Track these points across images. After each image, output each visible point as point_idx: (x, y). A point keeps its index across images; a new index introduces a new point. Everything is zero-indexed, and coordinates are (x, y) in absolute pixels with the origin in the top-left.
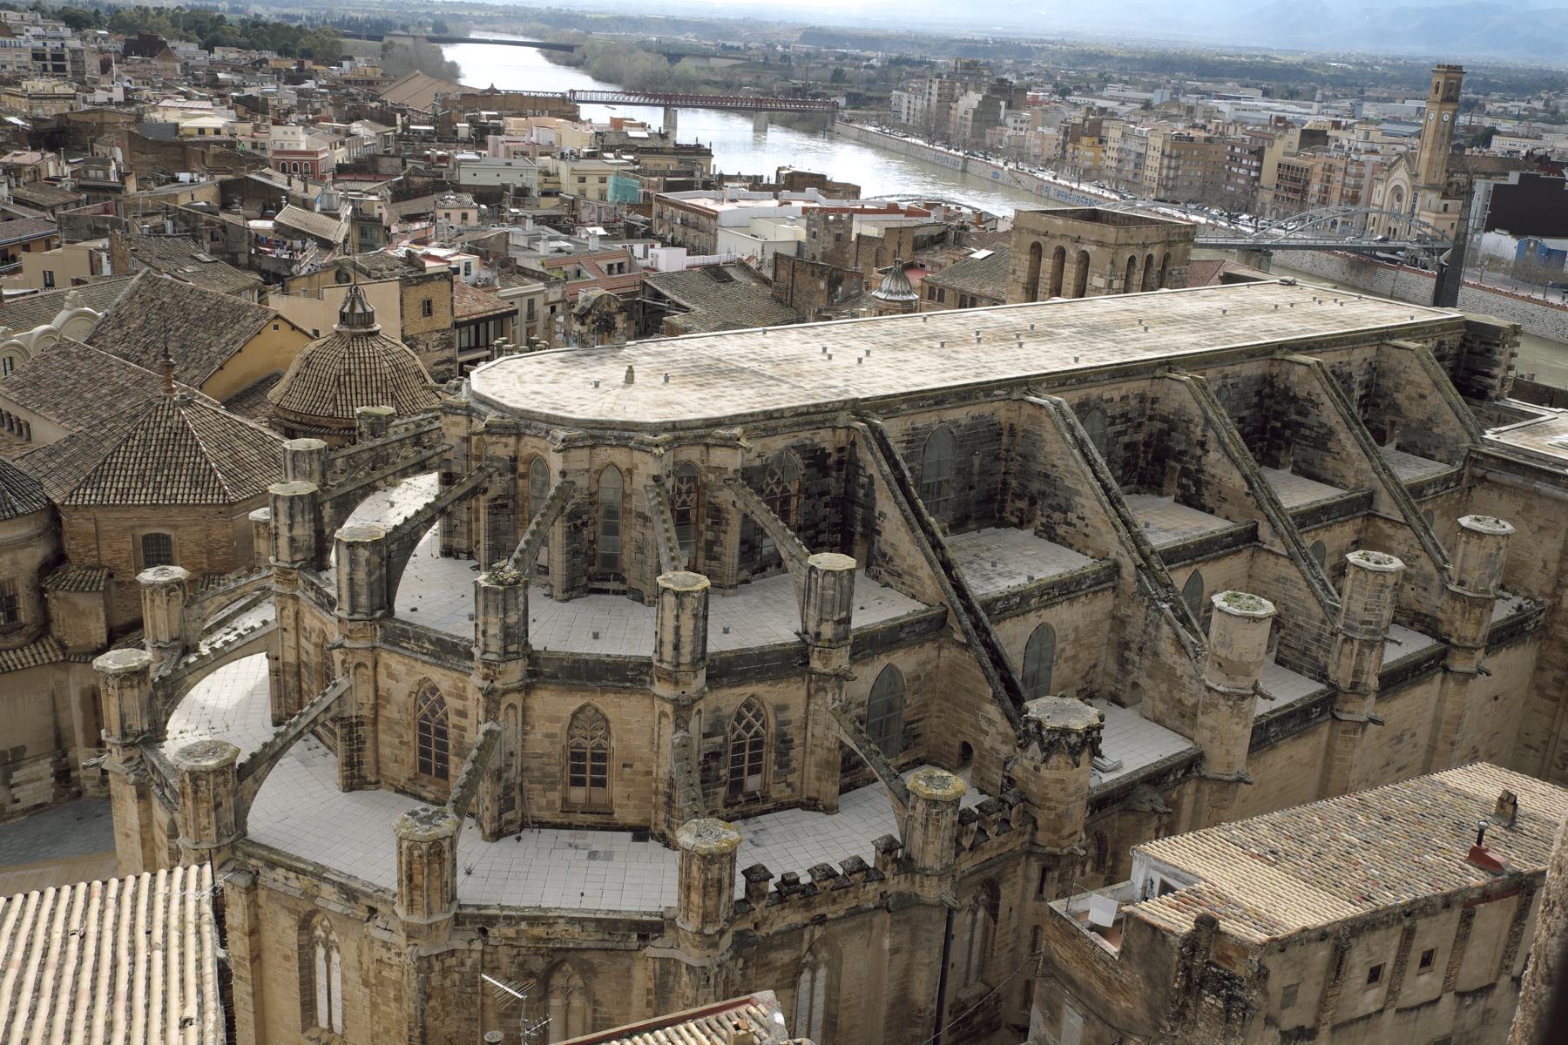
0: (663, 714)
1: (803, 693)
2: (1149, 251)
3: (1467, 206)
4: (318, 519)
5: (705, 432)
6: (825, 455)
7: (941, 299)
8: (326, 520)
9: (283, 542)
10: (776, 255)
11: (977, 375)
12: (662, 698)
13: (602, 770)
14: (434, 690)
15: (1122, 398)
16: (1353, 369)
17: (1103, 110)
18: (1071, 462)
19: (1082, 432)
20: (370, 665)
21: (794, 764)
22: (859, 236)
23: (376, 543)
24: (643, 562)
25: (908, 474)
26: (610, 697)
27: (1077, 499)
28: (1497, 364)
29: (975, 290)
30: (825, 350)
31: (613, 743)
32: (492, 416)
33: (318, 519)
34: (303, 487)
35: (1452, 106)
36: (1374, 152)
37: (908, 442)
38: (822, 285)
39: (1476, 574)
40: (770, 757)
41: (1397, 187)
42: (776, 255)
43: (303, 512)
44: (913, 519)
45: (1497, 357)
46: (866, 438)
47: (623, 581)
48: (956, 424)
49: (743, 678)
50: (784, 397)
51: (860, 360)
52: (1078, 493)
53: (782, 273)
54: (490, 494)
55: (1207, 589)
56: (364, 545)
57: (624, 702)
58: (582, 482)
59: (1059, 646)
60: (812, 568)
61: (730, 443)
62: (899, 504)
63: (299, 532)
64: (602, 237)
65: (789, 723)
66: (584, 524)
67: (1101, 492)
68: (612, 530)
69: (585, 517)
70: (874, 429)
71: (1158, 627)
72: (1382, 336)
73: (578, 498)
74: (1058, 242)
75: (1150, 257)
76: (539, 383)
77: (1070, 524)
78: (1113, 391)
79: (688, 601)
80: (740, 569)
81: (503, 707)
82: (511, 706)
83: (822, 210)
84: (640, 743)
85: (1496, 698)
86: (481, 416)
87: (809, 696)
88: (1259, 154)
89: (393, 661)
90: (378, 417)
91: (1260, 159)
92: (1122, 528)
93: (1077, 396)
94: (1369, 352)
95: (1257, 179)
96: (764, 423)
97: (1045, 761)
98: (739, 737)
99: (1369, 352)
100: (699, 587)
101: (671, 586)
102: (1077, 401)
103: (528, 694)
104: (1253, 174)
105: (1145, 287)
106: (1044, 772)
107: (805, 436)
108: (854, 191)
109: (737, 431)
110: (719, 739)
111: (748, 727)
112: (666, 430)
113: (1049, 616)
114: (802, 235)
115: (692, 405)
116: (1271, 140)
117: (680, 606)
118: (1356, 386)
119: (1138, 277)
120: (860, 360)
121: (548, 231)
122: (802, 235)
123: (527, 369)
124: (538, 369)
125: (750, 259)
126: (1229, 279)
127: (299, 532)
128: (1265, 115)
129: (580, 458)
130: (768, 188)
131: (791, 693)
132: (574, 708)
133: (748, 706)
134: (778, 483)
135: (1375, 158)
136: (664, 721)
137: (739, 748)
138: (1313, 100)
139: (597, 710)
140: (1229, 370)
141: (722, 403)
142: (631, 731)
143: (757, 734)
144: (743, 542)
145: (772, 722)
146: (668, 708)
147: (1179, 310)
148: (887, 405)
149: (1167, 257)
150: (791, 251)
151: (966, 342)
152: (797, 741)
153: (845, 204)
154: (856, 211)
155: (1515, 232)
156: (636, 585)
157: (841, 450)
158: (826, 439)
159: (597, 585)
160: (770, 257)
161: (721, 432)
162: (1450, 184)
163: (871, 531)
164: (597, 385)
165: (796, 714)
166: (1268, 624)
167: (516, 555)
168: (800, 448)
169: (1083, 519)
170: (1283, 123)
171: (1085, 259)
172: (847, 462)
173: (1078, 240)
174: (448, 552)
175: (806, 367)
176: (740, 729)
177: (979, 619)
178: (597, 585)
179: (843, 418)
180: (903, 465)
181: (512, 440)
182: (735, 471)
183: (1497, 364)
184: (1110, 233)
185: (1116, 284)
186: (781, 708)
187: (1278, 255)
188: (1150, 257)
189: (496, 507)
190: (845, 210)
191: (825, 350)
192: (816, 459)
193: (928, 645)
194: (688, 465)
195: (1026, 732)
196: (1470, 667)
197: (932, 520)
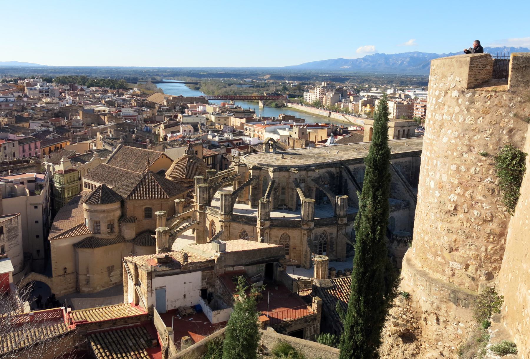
0: (305, 234)
1: (336, 230)
2: (404, 128)
4: (209, 193)
5: (307, 168)
8: (211, 193)
12: (304, 229)
13: (288, 250)
14: (245, 231)
15: (405, 162)
17: (372, 96)
18: (395, 176)
20: (228, 226)
21: (334, 249)
23: (231, 195)
24: (293, 200)
26: (291, 230)
27: (397, 185)
31: (291, 243)
33: (209, 193)
40: (328, 247)
43: (206, 191)
46: (344, 169)
47: (287, 206)
49: (322, 225)
50: (321, 161)
52: (397, 184)
54: (253, 185)
56: (228, 195)
57: (294, 232)
58: (277, 180)
59: (396, 223)
61: (313, 170)
62: (354, 185)
63: (205, 196)
65: (333, 238)
67: (404, 184)
68: (283, 193)
75: (404, 130)
78: (403, 160)
79: (311, 204)
81: (265, 233)
82: (267, 233)
84: (297, 242)
87: (338, 231)
89: (235, 225)
90: (213, 172)
92: (410, 192)
96: (320, 166)
97: (398, 245)
98: (321, 242)
103: (270, 231)
106: (398, 248)
110: (317, 241)
111: (323, 239)
115: (301, 162)
117: (309, 205)
127: (205, 196)
129: (277, 173)
131: (332, 230)
132: (281, 234)
133: (323, 233)
134: (323, 181)
136: (304, 236)
137: (321, 245)
139: (287, 234)
141: (308, 162)
142: (295, 239)
143: (325, 241)
145: (329, 237)
146: (306, 232)
147: (415, 142)
149: (409, 130)
151: (362, 149)
152: (335, 243)
156: (290, 206)
157: (338, 173)
158: (333, 170)
159: (280, 207)
165: (335, 235)
168: (328, 172)
175: (324, 155)
176: (321, 240)
178: (280, 207)
181: (258, 171)
186: (331, 234)
188: (404, 130)
189: (254, 188)
195: (393, 238)
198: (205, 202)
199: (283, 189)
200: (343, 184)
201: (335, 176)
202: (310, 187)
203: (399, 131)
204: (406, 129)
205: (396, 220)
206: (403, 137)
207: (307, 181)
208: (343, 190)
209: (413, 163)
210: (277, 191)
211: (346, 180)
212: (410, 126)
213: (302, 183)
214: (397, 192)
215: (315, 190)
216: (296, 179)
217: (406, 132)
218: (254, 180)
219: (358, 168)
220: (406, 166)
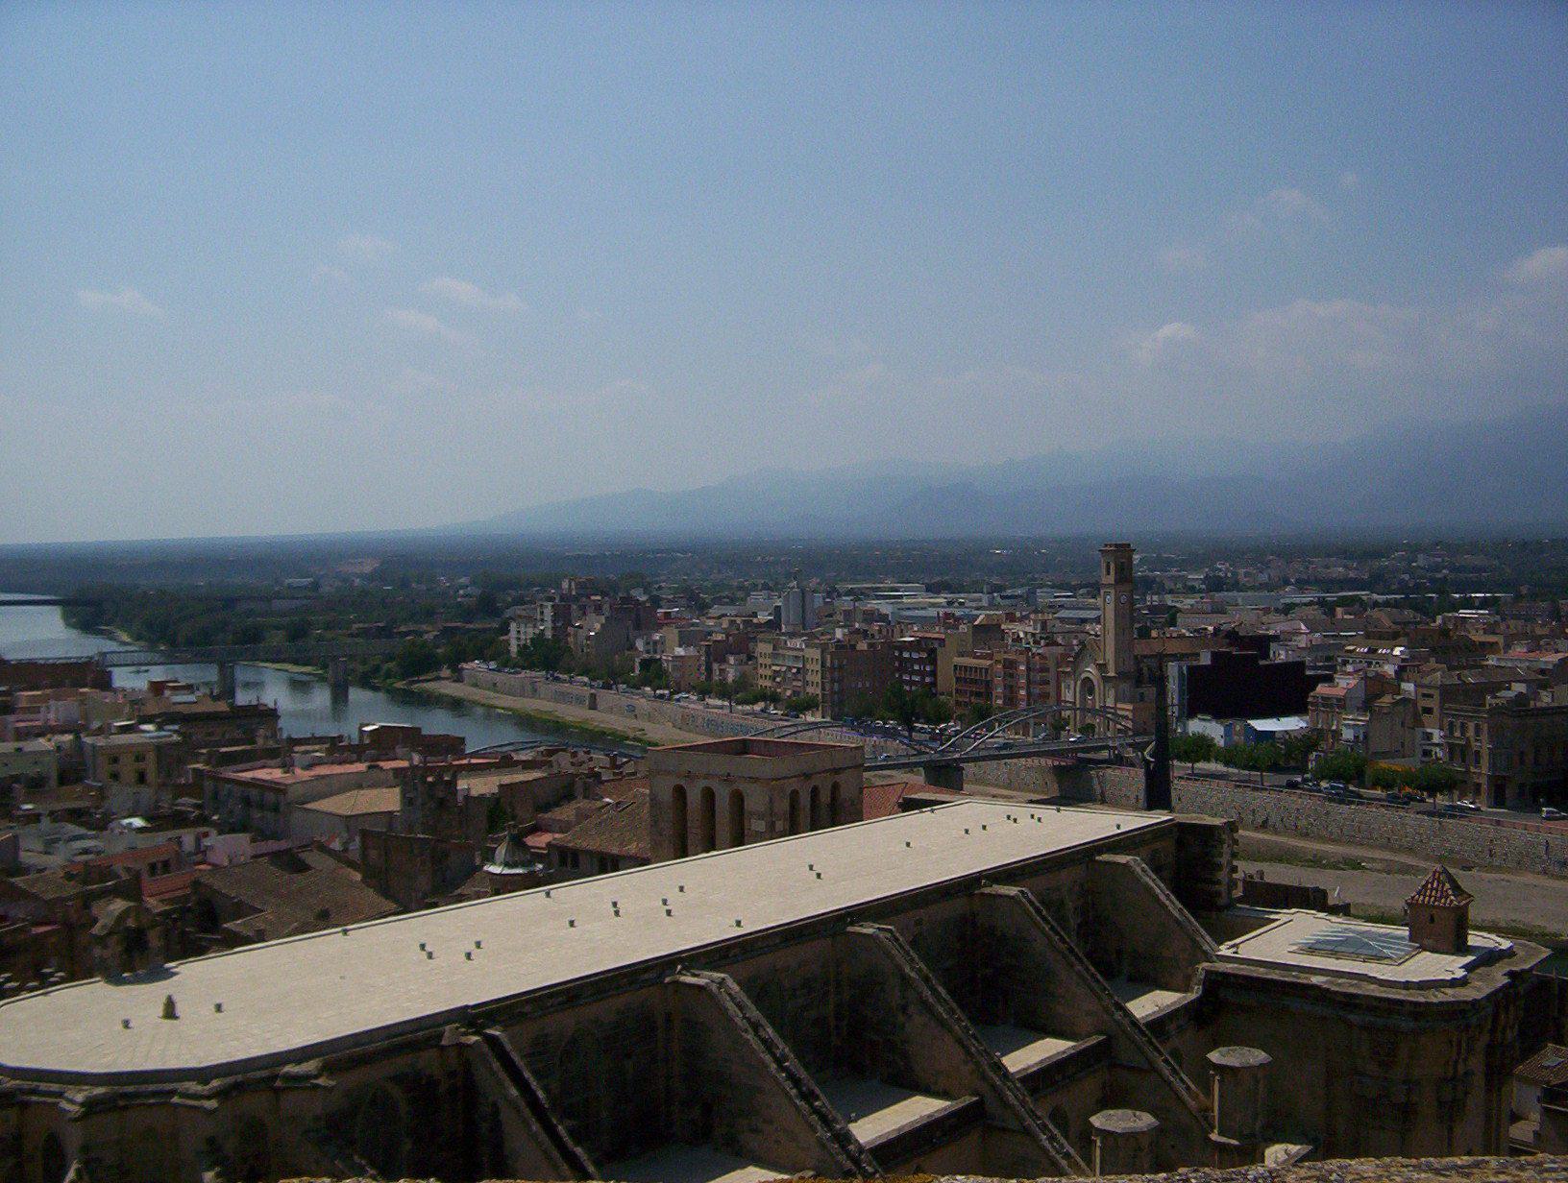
3: (1162, 692)
7: (576, 864)
25: (541, 1094)
28: (1219, 867)
29: (615, 851)
44: (556, 1154)
51: (468, 956)
53: (373, 854)
64: (140, 830)
70: (492, 1041)
74: (702, 783)
75: (815, 791)
95: (934, 684)
104: (928, 680)
105: (815, 825)
108: (455, 745)
109: (310, 1066)
119: (804, 816)
120: (468, 956)
121: (72, 829)
126: (909, 805)
130: (350, 748)
149: (835, 787)
155: (1218, 715)
157: (452, 1074)
158: (428, 1061)
168: (396, 1079)
171: (738, 799)
172: (466, 1088)
182: (317, 1118)
183: (1219, 867)
185: (779, 825)
187: (970, 768)
192: (420, 1088)
197: (579, 1150)
200: (484, 1126)
203: (795, 794)
211: (495, 1105)
216: (211, 1141)
217: (825, 797)
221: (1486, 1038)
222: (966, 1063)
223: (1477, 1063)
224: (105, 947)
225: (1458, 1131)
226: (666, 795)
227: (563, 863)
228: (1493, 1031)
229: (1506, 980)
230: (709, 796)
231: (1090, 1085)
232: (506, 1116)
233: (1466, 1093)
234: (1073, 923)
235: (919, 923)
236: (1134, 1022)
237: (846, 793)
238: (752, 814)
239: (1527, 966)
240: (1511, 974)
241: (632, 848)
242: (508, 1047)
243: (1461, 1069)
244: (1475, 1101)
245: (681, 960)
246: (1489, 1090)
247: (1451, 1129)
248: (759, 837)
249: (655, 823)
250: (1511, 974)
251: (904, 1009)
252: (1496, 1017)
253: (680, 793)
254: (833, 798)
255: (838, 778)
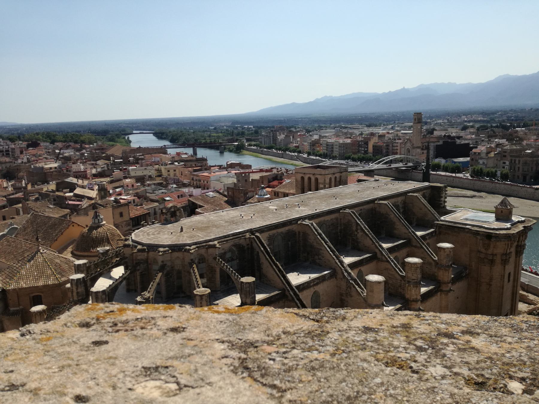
3: (428, 153)
6: (243, 247)
7: (278, 196)
9: (75, 294)
10: (228, 188)
11: (286, 217)
15: (331, 220)
16: (399, 203)
19: (320, 231)
22: (252, 179)
25: (269, 250)
28: (442, 197)
29: (287, 192)
30: (241, 215)
32: (139, 247)
34: (80, 276)
35: (419, 124)
36: (400, 139)
37: (268, 240)
38: (242, 195)
39: (445, 261)
41: (408, 149)
42: (228, 188)
45: (442, 195)
48: (282, 233)
51: (252, 217)
52: (321, 250)
53: (230, 193)
55: (364, 275)
58: (169, 264)
59: (321, 297)
60: (242, 282)
63: (79, 290)
66: (171, 277)
69: (171, 274)
70: (257, 237)
71: (350, 288)
72: (405, 193)
73: (168, 269)
74: (308, 176)
75: (336, 178)
76: (154, 234)
77: (320, 259)
78: (328, 218)
79: (204, 297)
80: (221, 285)
83: (240, 173)
85: (458, 298)
86: (136, 247)
88: (366, 143)
91: (367, 145)
93: (318, 220)
94: (403, 198)
95: (367, 150)
96: (222, 239)
99: (403, 198)
100: (207, 292)
101: (198, 293)
102: (318, 222)
104: (366, 149)
107: (237, 241)
108: (249, 167)
109: (216, 242)
112: (193, 245)
113: (317, 288)
114: (235, 181)
116: (369, 139)
118: (401, 208)
120: (252, 217)
122: (235, 181)
123: (151, 230)
124: (153, 230)
125: (220, 190)
126: (359, 181)
127: (79, 290)
128: (367, 132)
130: (224, 168)
135: (400, 141)
138: (380, 126)
140: (362, 207)
144: (221, 276)
148: (261, 230)
149: (341, 176)
150: (232, 186)
153: (247, 171)
154: (251, 172)
155: (445, 158)
157: (248, 245)
158: (242, 242)
160: (226, 188)
161: (211, 243)
162: (423, 146)
163: (260, 268)
164: (172, 233)
166: (383, 284)
167: (149, 289)
168: (235, 245)
169: (323, 257)
170: (372, 134)
171: (317, 180)
173: (314, 174)
174: (128, 290)
177: (295, 292)
179: (248, 235)
180: (267, 247)
183: (442, 197)
184: (323, 171)
185: (327, 186)
187: (376, 172)
190: (247, 172)
191: (241, 215)
192: (239, 247)
193: (281, 302)
194: (201, 255)
196: (448, 289)
197: (278, 263)
198: (80, 298)
199: (179, 272)
200: (256, 257)
201: (246, 248)
202: (212, 267)
204: (338, 175)
205: (321, 294)
206: (336, 186)
207: (208, 261)
208: (256, 264)
209: (341, 220)
210: (171, 277)
211: (258, 252)
212: (341, 173)
213: (203, 263)
214: (321, 258)
215: (218, 270)
217: (338, 179)
218: (141, 265)
219: (274, 235)
220: (332, 224)
221: (516, 244)
222: (372, 244)
223: (513, 250)
224: (167, 215)
225: (507, 267)
226: (299, 179)
227: (275, 195)
228: (518, 242)
229: (523, 228)
230: (310, 179)
231: (404, 251)
232: (261, 254)
233: (510, 258)
234: (401, 211)
235: (361, 210)
236: (417, 236)
237: (343, 178)
238: (320, 183)
239: (529, 225)
240: (524, 227)
241: (291, 191)
242: (261, 238)
243: (508, 251)
244: (512, 259)
245: (302, 218)
246: (516, 257)
247: (505, 267)
248: (322, 189)
249: (296, 186)
250: (524, 227)
251: (357, 231)
252: (519, 238)
253: (303, 178)
254: (340, 179)
255: (341, 174)
